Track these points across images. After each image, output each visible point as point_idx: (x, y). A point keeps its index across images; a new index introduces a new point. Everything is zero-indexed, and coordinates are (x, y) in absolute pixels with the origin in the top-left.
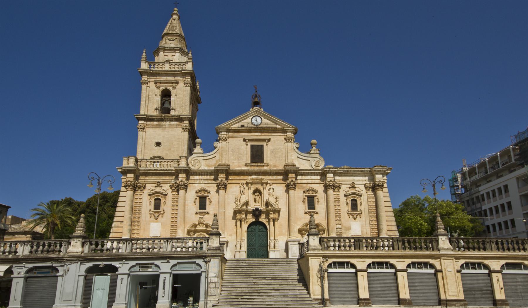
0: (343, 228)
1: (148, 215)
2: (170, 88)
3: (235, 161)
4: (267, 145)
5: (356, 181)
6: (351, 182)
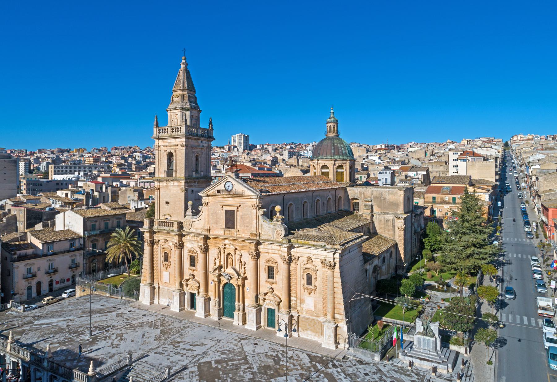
1: (162, 266)
3: (214, 225)
4: (238, 211)
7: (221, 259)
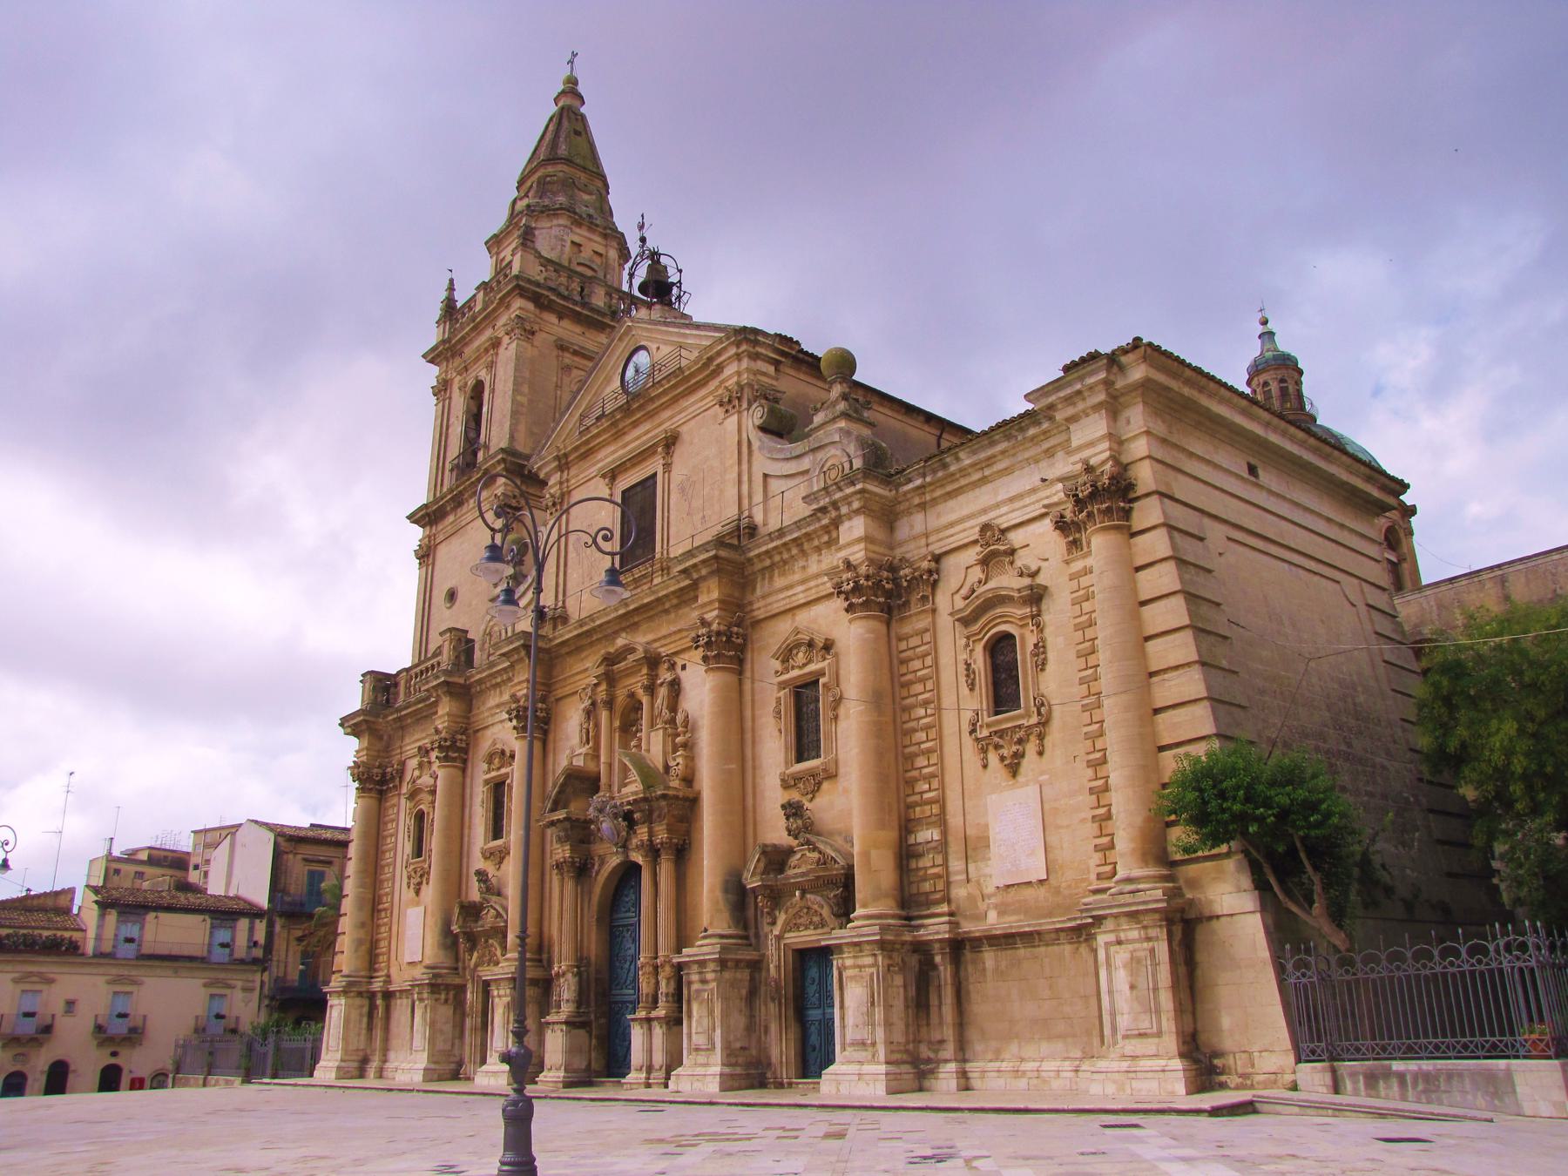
0: (955, 848)
2: (483, 375)
5: (1004, 509)
6: (978, 529)
7: (597, 748)
